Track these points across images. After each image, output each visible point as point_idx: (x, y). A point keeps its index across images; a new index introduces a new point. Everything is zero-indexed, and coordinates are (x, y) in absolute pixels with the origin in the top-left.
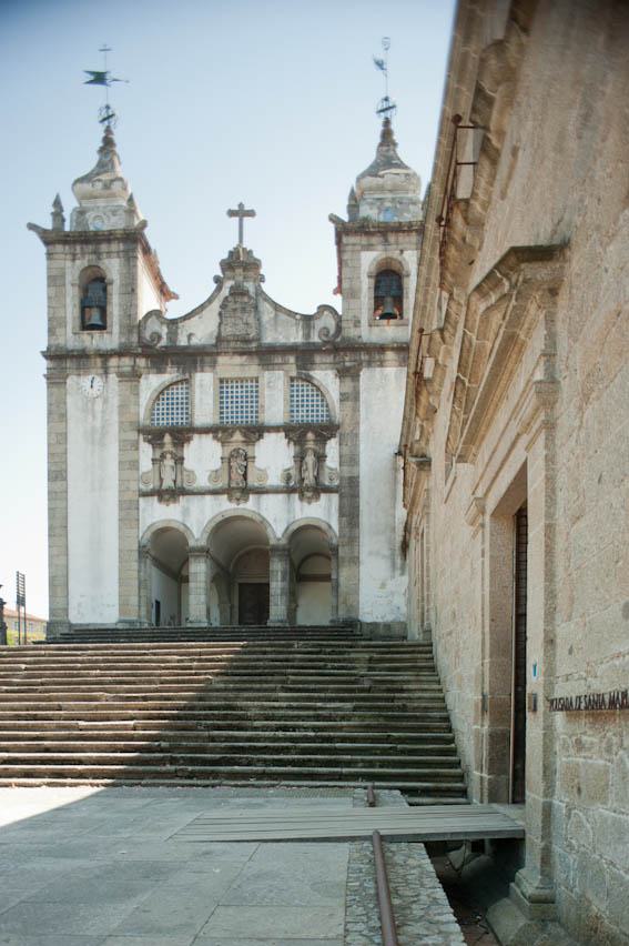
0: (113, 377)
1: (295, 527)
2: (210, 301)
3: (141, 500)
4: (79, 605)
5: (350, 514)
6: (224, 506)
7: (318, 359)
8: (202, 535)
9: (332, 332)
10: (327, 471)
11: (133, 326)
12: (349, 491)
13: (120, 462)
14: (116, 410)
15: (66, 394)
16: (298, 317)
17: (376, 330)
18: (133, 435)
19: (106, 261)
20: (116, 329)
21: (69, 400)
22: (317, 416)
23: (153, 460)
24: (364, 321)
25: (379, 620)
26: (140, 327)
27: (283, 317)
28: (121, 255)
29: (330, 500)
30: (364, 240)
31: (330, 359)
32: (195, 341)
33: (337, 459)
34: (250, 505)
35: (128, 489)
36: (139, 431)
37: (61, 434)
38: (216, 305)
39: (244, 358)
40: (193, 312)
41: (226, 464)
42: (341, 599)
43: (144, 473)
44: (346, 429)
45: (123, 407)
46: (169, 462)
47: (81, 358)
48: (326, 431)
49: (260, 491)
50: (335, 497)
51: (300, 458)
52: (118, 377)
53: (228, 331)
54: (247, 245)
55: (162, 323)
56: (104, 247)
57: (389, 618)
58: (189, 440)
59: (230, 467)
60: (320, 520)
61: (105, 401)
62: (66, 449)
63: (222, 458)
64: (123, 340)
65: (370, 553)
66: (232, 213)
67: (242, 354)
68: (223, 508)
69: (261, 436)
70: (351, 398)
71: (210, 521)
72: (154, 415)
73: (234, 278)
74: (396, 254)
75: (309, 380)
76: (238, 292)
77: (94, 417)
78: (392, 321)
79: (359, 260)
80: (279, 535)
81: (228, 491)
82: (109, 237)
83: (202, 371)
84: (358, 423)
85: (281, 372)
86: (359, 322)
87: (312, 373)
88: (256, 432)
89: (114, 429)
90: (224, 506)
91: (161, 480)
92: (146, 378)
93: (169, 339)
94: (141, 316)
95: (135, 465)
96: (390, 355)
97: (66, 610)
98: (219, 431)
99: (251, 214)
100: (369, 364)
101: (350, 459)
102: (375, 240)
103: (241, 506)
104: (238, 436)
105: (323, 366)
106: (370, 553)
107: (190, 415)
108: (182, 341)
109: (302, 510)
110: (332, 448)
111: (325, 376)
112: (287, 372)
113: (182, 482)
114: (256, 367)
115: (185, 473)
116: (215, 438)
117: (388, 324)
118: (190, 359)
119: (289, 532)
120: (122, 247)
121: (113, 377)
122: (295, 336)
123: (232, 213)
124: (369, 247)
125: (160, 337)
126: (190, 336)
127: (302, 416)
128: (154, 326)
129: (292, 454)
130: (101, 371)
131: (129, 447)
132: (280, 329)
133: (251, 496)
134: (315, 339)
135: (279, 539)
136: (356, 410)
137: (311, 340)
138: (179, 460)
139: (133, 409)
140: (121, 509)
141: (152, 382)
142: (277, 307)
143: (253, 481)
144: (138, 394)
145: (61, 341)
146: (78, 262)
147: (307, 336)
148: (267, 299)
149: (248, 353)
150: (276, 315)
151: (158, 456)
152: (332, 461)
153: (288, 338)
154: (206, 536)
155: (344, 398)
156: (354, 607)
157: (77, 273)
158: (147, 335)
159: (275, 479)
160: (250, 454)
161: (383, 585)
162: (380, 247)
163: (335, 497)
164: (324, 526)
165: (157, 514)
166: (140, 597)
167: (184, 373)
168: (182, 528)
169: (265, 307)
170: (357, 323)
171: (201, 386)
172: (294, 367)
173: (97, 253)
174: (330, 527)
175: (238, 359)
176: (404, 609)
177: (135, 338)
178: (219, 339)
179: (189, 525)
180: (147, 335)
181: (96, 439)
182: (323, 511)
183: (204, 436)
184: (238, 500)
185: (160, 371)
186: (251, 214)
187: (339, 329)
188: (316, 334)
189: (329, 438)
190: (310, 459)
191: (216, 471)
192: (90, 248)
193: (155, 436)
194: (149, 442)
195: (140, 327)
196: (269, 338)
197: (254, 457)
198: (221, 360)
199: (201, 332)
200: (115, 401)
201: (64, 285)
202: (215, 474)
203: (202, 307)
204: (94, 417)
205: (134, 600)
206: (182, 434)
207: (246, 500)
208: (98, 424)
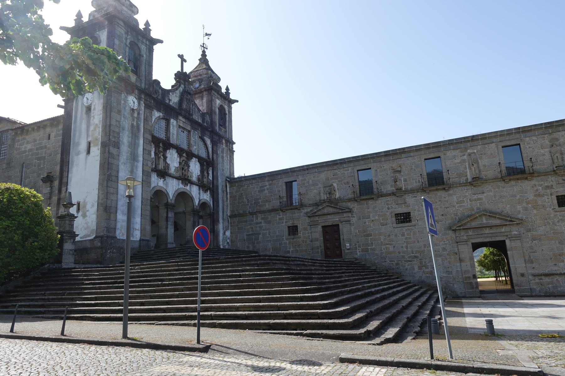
34: (188, 188)
68: (180, 187)
88: (191, 155)
138: (165, 158)
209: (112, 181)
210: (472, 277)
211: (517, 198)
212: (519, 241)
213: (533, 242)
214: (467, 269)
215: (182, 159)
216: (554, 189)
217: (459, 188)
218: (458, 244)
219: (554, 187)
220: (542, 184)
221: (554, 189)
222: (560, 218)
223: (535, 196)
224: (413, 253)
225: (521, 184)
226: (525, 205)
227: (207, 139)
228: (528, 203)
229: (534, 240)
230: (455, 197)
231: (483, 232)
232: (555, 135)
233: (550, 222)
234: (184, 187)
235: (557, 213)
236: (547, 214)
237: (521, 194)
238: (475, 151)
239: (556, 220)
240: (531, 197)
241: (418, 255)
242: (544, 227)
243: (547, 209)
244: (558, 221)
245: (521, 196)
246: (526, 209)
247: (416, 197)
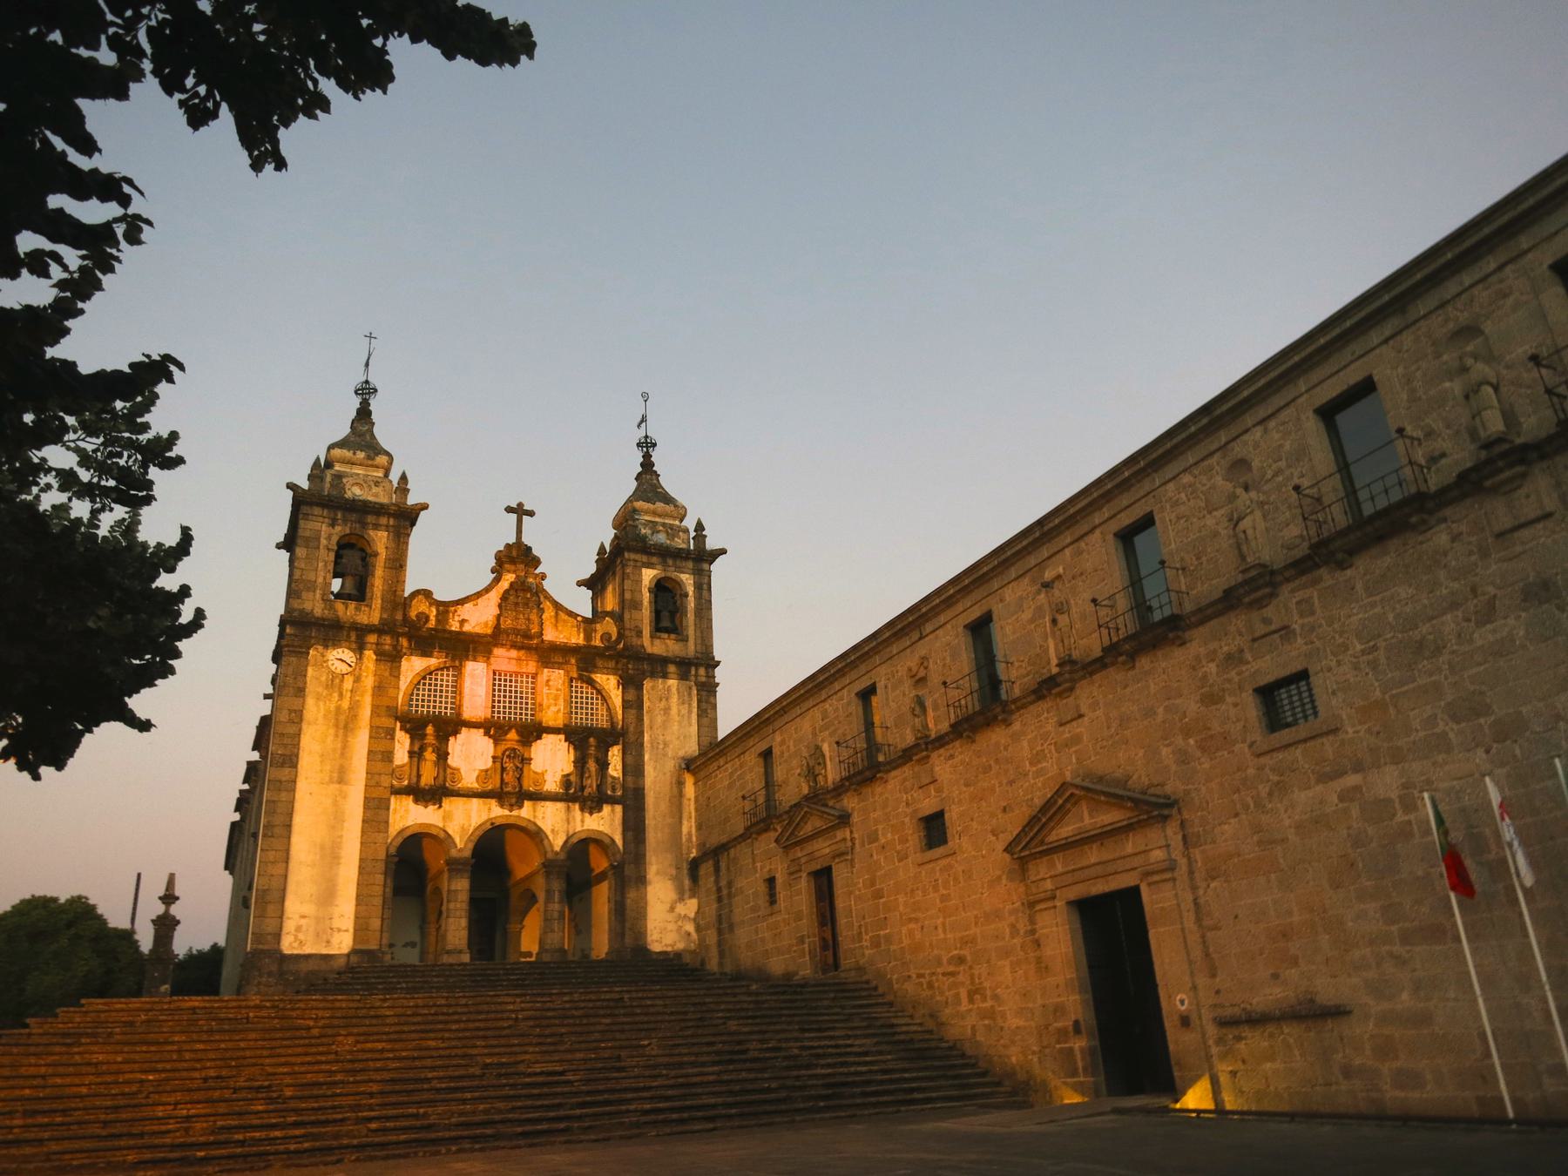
0: (369, 654)
1: (575, 840)
2: (487, 590)
3: (393, 799)
4: (299, 929)
5: (634, 825)
6: (496, 811)
7: (600, 663)
8: (466, 844)
9: (614, 638)
10: (610, 780)
11: (397, 602)
12: (633, 802)
13: (370, 752)
14: (370, 692)
15: (307, 666)
16: (579, 619)
17: (657, 642)
18: (387, 722)
19: (371, 533)
20: (377, 603)
21: (310, 671)
22: (601, 721)
23: (409, 752)
24: (646, 632)
25: (669, 949)
26: (406, 603)
27: (562, 615)
28: (391, 529)
29: (613, 811)
30: (644, 559)
31: (612, 664)
32: (467, 628)
33: (619, 767)
34: (526, 811)
35: (378, 785)
36: (397, 718)
37: (295, 711)
38: (494, 597)
39: (522, 652)
40: (468, 597)
41: (498, 765)
42: (628, 925)
43: (398, 767)
44: (631, 737)
45: (379, 689)
46: (430, 755)
47: (332, 632)
48: (608, 737)
49: (538, 797)
50: (619, 809)
51: (580, 763)
52: (375, 653)
53: (507, 623)
54: (526, 540)
55: (431, 605)
56: (370, 519)
57: (680, 946)
58: (456, 733)
59: (503, 769)
60: (601, 832)
61: (357, 680)
62: (300, 730)
63: (494, 757)
64: (385, 616)
65: (658, 873)
66: (509, 510)
67: (519, 648)
68: (493, 815)
69: (539, 737)
70: (634, 705)
71: (476, 829)
72: (412, 700)
73: (514, 572)
74: (674, 575)
75: (591, 682)
76: (518, 587)
77: (341, 695)
78: (673, 636)
79: (640, 574)
80: (557, 848)
81: (499, 795)
82: (378, 510)
83: (475, 660)
84: (642, 733)
85: (562, 672)
86: (642, 632)
87: (593, 676)
88: (533, 732)
89: (366, 712)
90: (496, 811)
91: (419, 776)
92: (409, 660)
93: (438, 621)
94: (406, 595)
95: (388, 756)
96: (672, 668)
97: (278, 936)
98: (493, 728)
99: (531, 514)
100: (653, 675)
101: (634, 768)
102: (654, 559)
103: (515, 813)
104: (513, 735)
105: (605, 671)
106: (658, 873)
107: (458, 708)
108: (454, 626)
109: (583, 821)
110: (615, 755)
111: (609, 683)
112: (567, 672)
113: (445, 780)
114: (535, 664)
115: (449, 771)
116: (487, 734)
117: (669, 638)
118: (462, 647)
119: (568, 845)
120: (392, 522)
121: (369, 654)
122: (578, 639)
123: (509, 510)
124: (649, 566)
125: (427, 619)
126: (463, 622)
127: (580, 719)
128: (418, 607)
129: (572, 758)
130: (354, 646)
131: (382, 736)
132: (560, 628)
133: (527, 804)
134: (597, 642)
135: (557, 853)
136: (640, 719)
137: (593, 643)
138: (443, 756)
139: (391, 692)
140: (366, 807)
141: (413, 666)
142: (558, 607)
143: (529, 786)
144: (398, 677)
145: (308, 606)
146: (338, 528)
147: (588, 637)
148: (548, 597)
149: (528, 648)
150: (557, 614)
151: (416, 749)
152: (615, 769)
153: (569, 639)
154: (471, 846)
155: (626, 705)
156: (641, 934)
157: (335, 539)
158: (413, 614)
159: (552, 784)
160: (526, 756)
161: (672, 909)
162: (659, 567)
163: (619, 809)
164: (607, 841)
165: (408, 815)
166: (383, 920)
167: (453, 660)
168: (442, 835)
169: (547, 605)
170: (639, 633)
171: (473, 676)
172: (575, 668)
173: (364, 525)
174: (613, 841)
175: (514, 653)
176: (694, 936)
177: (399, 617)
178: (497, 627)
179: (450, 832)
180: (413, 614)
181: (344, 724)
182: (606, 822)
183: (473, 731)
184: (512, 805)
185: (426, 653)
186: (531, 514)
187: (621, 636)
188: (598, 637)
189: (612, 745)
190: (592, 766)
191: (487, 771)
192: (354, 516)
193: (415, 726)
194: (407, 731)
195: (406, 603)
196: (550, 635)
197: (531, 759)
198: (498, 651)
199: (478, 618)
200: (369, 681)
201: (318, 548)
202: (484, 775)
203: (479, 595)
204: (341, 695)
205: (376, 923)
206: (450, 726)
207: (521, 807)
208: (345, 704)
209: (272, 836)
210: (1071, 1028)
211: (1160, 718)
212: (1170, 884)
213: (1208, 886)
214: (1059, 1000)
215: (502, 747)
216: (1248, 663)
217: (1032, 707)
218: (1038, 907)
219: (1248, 656)
220: (1215, 651)
221: (1248, 663)
222: (1275, 778)
223: (1202, 701)
224: (956, 949)
225: (1164, 665)
226: (1179, 740)
227: (605, 677)
228: (1187, 733)
229: (1213, 878)
230: (1025, 744)
231: (1085, 863)
232: (1238, 450)
233: (1249, 799)
234: (506, 812)
235: (1263, 760)
236: (1239, 770)
237: (1166, 703)
238: (1061, 570)
239: (1263, 790)
240: (1192, 707)
241: (965, 952)
242: (1232, 821)
243: (1237, 748)
244: (1270, 794)
245: (1167, 709)
246: (1183, 758)
247: (952, 757)
